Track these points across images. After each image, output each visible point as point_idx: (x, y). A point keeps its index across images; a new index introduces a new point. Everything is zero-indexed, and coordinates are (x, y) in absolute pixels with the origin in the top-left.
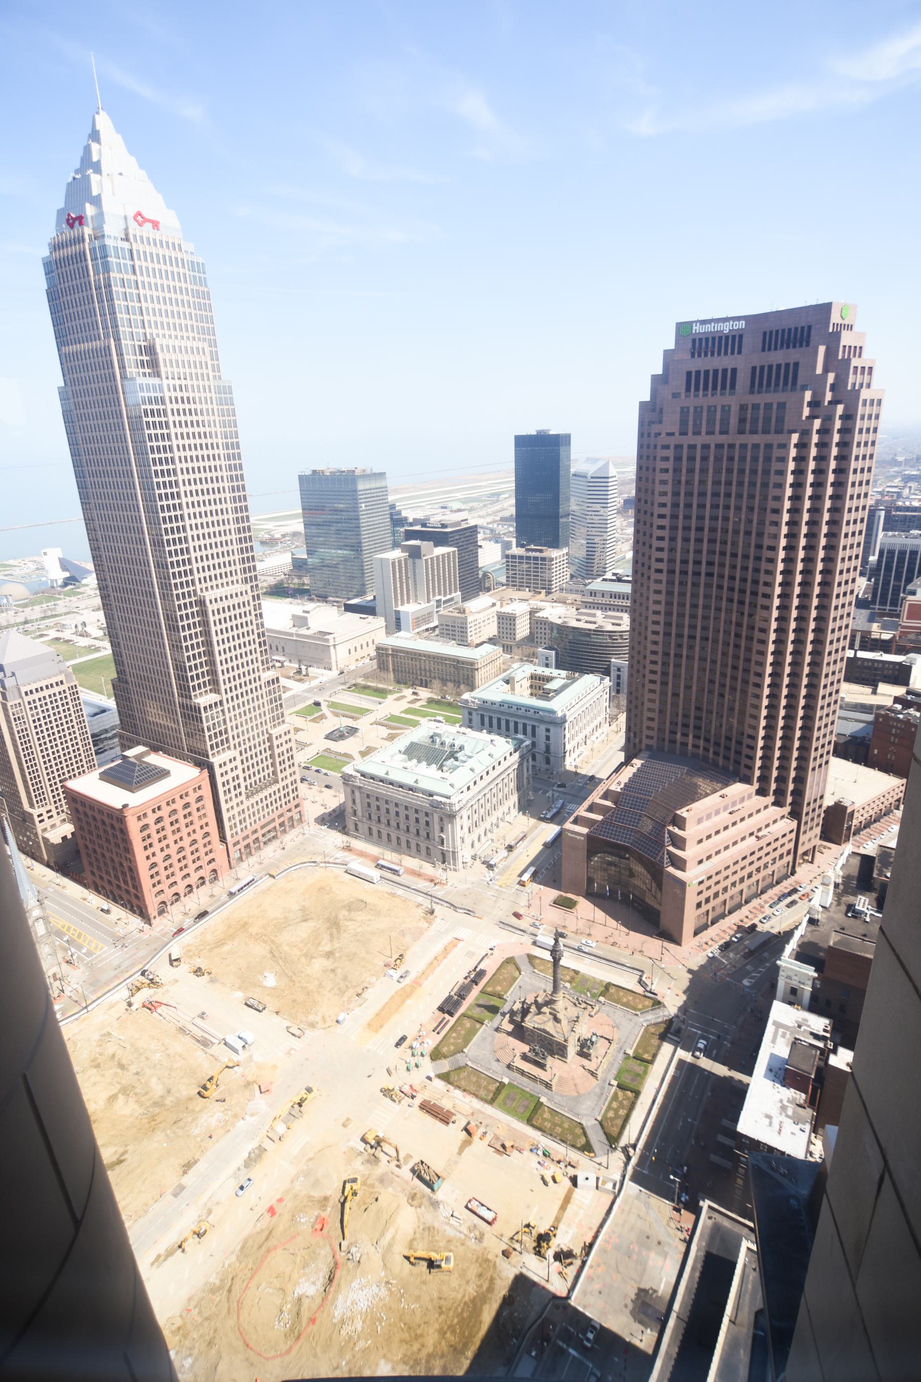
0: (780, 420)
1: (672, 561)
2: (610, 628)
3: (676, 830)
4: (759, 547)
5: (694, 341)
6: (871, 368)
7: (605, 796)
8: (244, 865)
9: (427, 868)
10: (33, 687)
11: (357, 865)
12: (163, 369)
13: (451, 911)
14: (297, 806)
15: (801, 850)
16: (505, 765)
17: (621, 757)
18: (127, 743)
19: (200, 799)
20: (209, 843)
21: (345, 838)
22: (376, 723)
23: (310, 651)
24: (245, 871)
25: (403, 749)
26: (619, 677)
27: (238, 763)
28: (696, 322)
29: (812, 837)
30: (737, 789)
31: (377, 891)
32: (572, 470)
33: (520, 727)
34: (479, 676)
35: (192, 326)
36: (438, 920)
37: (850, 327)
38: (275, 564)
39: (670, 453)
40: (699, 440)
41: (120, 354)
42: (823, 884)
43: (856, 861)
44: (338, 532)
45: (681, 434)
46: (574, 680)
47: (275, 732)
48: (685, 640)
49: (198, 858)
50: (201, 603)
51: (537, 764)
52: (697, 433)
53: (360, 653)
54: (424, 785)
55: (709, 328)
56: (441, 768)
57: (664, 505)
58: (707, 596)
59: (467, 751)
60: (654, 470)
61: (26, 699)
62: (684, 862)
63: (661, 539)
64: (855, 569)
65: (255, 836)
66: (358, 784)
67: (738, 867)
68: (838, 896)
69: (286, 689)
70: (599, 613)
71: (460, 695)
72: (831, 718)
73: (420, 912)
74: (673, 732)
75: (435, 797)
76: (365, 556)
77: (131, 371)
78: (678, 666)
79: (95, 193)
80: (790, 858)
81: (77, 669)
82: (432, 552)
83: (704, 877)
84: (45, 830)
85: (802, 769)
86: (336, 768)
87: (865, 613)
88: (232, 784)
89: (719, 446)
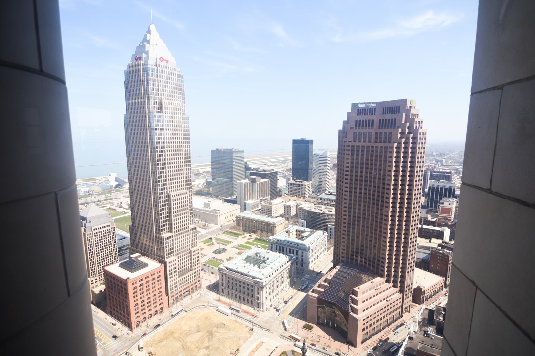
0: (390, 138)
1: (351, 188)
2: (327, 212)
3: (354, 297)
4: (384, 184)
5: (358, 110)
6: (422, 122)
7: (325, 281)
8: (175, 306)
9: (251, 310)
10: (97, 227)
11: (222, 308)
12: (164, 110)
13: (260, 329)
14: (199, 281)
15: (404, 307)
16: (285, 266)
17: (331, 265)
18: (132, 252)
19: (159, 276)
20: (161, 296)
21: (218, 295)
22: (234, 247)
23: (209, 217)
24: (175, 309)
26: (331, 232)
27: (177, 262)
29: (409, 301)
30: (378, 280)
31: (230, 320)
32: (314, 153)
33: (292, 251)
34: (276, 229)
36: (254, 333)
37: (414, 108)
38: (199, 183)
39: (350, 148)
40: (360, 144)
41: (149, 104)
42: (414, 322)
43: (427, 312)
44: (224, 172)
46: (313, 233)
47: (193, 249)
48: (357, 218)
49: (156, 302)
50: (169, 196)
51: (298, 266)
52: (360, 142)
53: (230, 219)
54: (252, 274)
55: (363, 106)
56: (259, 267)
57: (348, 167)
58: (364, 202)
59: (270, 260)
61: (94, 232)
62: (357, 310)
63: (347, 179)
64: (420, 193)
65: (181, 293)
66: (225, 272)
67: (379, 313)
68: (420, 327)
69: (199, 232)
70: (323, 206)
71: (268, 237)
72: (414, 252)
73: (247, 330)
74: (352, 255)
75: (256, 279)
76: (234, 181)
77: (152, 110)
78: (354, 228)
79: (146, 50)
80: (400, 310)
81: (116, 221)
83: (365, 317)
84: (93, 287)
85: (403, 272)
86: (217, 265)
87: (425, 210)
88: (173, 271)
89: (368, 147)
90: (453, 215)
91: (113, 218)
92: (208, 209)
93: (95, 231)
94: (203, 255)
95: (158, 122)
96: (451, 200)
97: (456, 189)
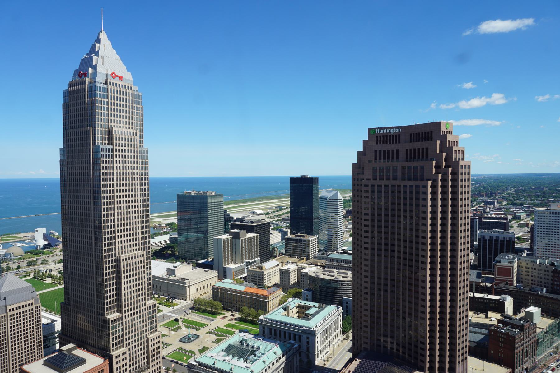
1: (373, 243)
4: (417, 237)
5: (377, 137)
6: (463, 151)
12: (114, 142)
22: (210, 332)
25: (224, 349)
28: (378, 128)
33: (292, 336)
34: (270, 304)
35: (132, 123)
37: (451, 133)
38: (162, 240)
39: (369, 189)
40: (383, 183)
41: (94, 134)
45: (373, 179)
47: (150, 337)
50: (118, 261)
53: (203, 291)
55: (384, 131)
56: (246, 361)
59: (262, 350)
60: (361, 197)
63: (367, 232)
64: (468, 249)
69: (160, 311)
76: (210, 237)
79: (94, 63)
82: (246, 236)
87: (475, 272)
89: (393, 186)
90: (515, 278)
91: (38, 293)
92: (172, 278)
93: (12, 313)
94: (166, 345)
95: (106, 157)
96: (511, 256)
97: (516, 240)
